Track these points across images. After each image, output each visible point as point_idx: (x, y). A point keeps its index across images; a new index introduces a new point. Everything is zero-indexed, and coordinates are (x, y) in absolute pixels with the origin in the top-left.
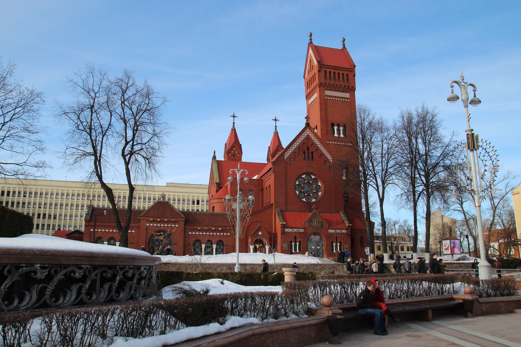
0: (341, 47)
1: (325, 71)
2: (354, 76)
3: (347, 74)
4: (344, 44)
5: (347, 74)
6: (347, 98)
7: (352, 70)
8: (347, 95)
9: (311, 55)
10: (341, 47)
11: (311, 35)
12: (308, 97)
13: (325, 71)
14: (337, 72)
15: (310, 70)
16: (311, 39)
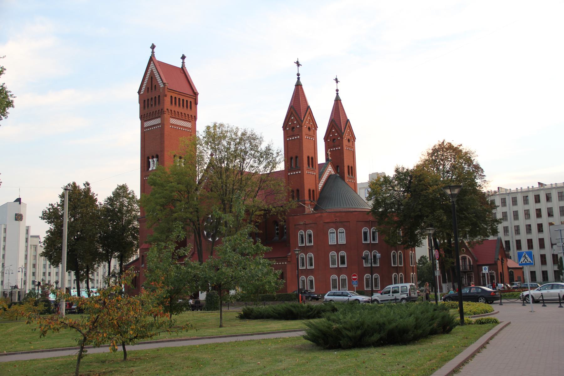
0: (180, 66)
1: (171, 97)
2: (196, 104)
3: (191, 102)
4: (183, 63)
5: (191, 102)
6: (189, 128)
7: (195, 98)
8: (188, 125)
9: (152, 71)
10: (180, 66)
11: (153, 47)
12: (144, 117)
13: (171, 97)
14: (182, 98)
15: (150, 90)
16: (153, 52)
